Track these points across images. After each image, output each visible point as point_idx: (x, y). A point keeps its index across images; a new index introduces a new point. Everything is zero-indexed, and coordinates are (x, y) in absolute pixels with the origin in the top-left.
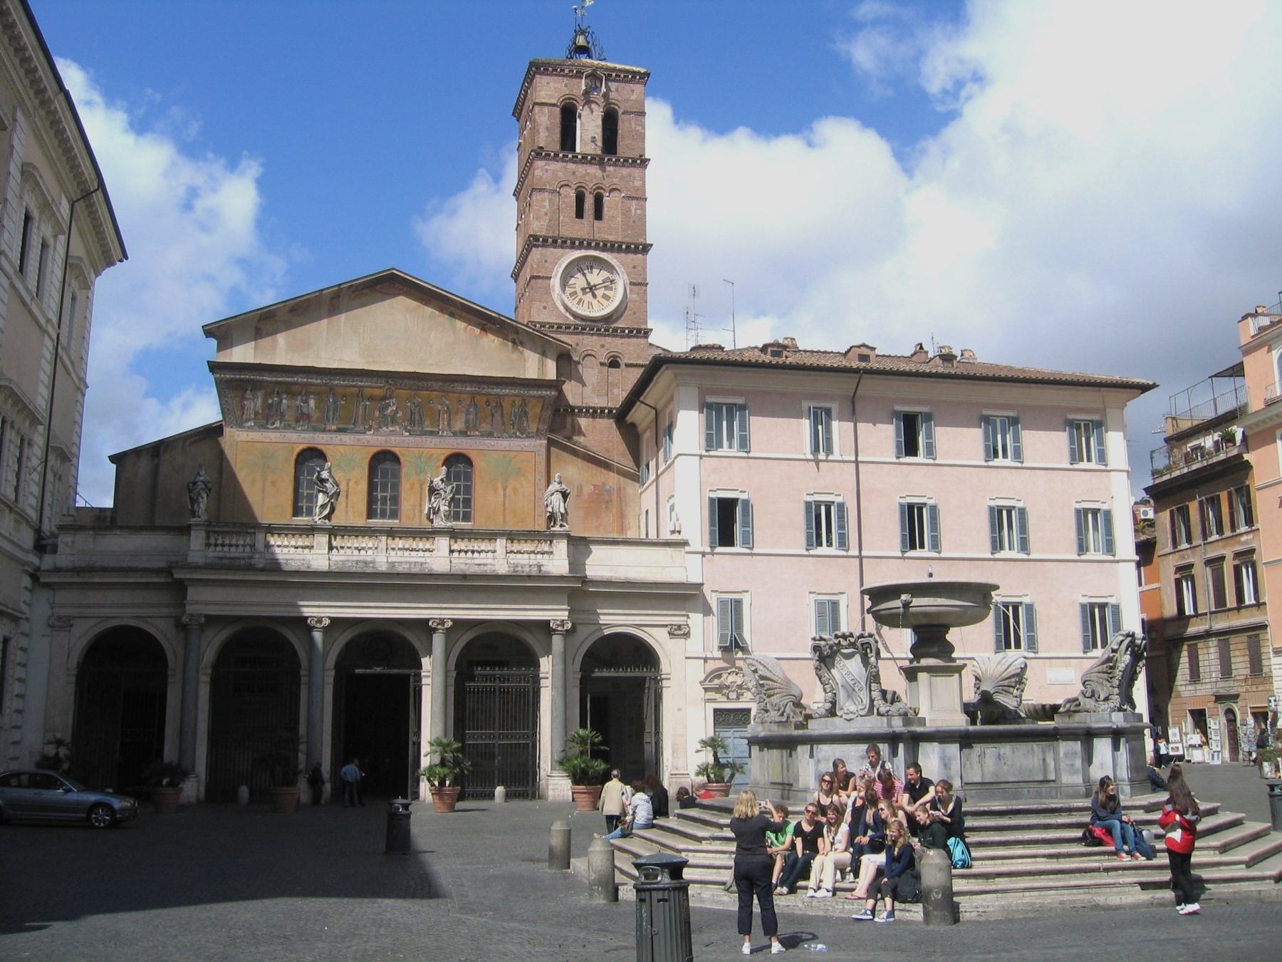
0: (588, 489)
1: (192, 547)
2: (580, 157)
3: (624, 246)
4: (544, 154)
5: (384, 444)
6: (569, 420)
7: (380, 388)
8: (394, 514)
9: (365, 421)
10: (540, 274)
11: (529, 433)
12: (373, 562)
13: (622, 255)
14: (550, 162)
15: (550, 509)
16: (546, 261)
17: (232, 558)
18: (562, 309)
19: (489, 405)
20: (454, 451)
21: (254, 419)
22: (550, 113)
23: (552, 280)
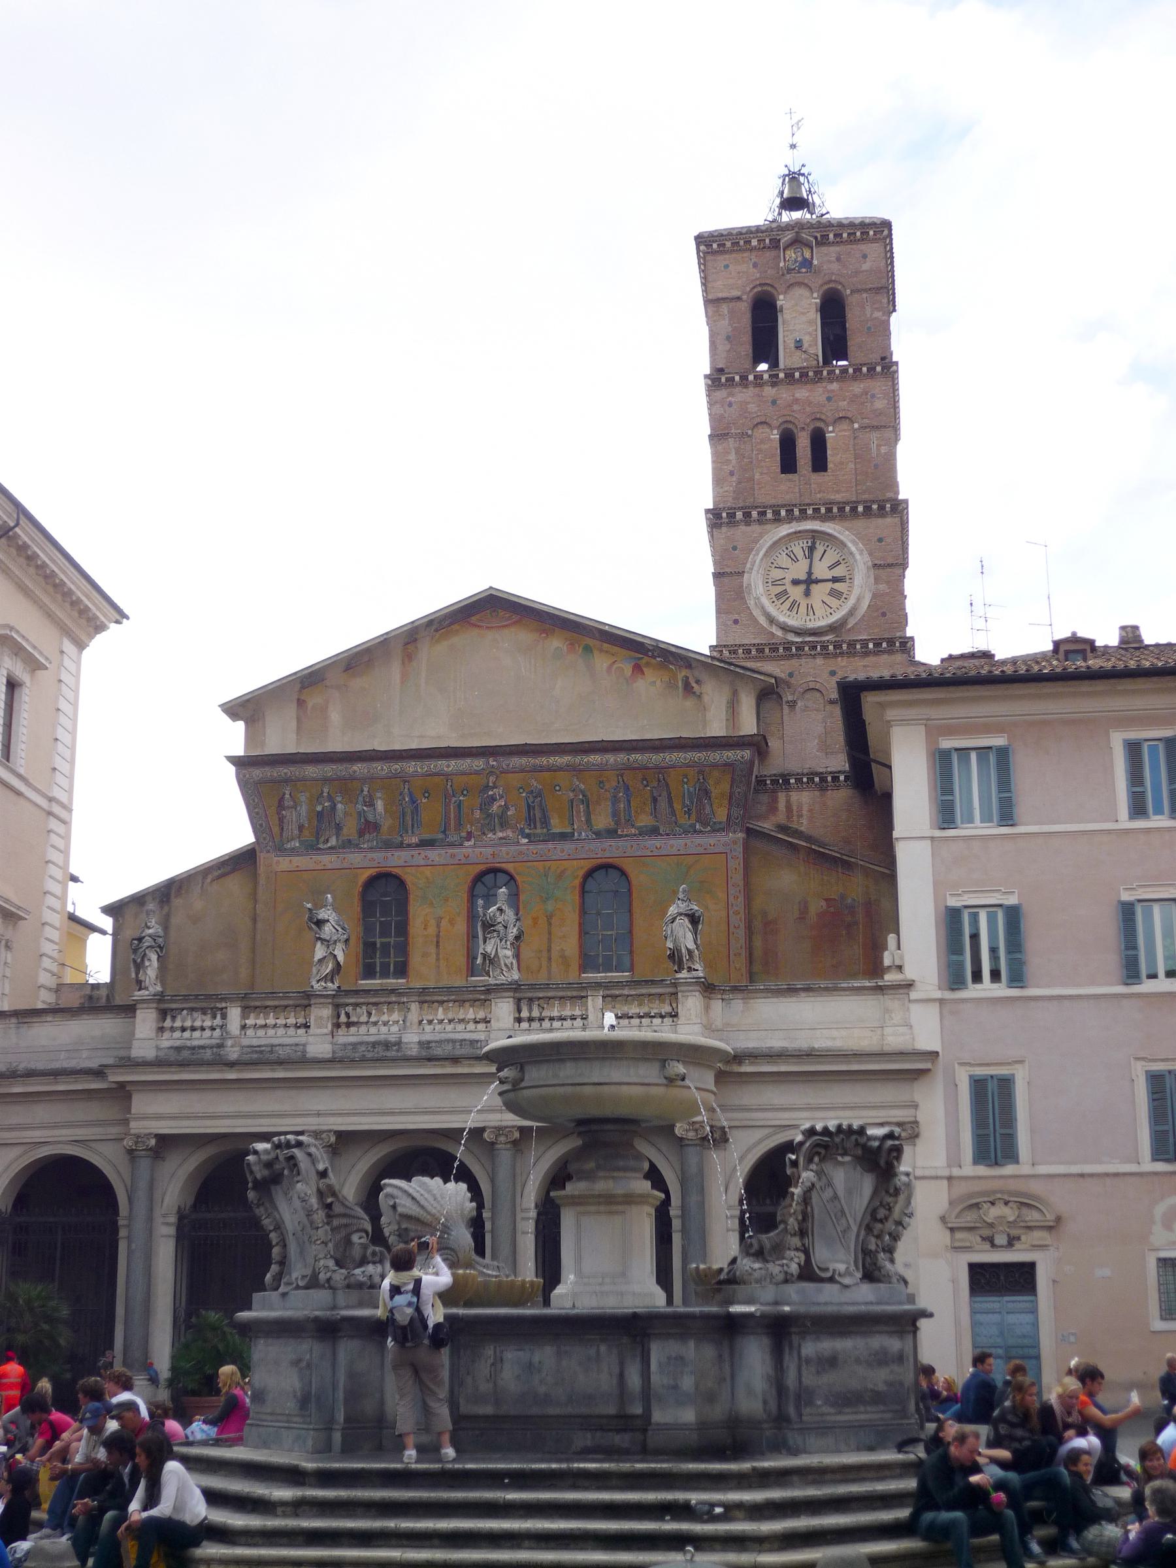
0: (816, 906)
1: (138, 1035)
2: (782, 375)
3: (860, 509)
4: (723, 380)
5: (491, 859)
6: (782, 797)
7: (477, 773)
8: (402, 970)
9: (459, 826)
10: (728, 570)
11: (715, 823)
12: (399, 1043)
13: (860, 523)
14: (737, 389)
15: (670, 945)
16: (735, 548)
17: (193, 1048)
18: (762, 620)
20: (600, 861)
21: (299, 837)
22: (732, 312)
23: (746, 575)
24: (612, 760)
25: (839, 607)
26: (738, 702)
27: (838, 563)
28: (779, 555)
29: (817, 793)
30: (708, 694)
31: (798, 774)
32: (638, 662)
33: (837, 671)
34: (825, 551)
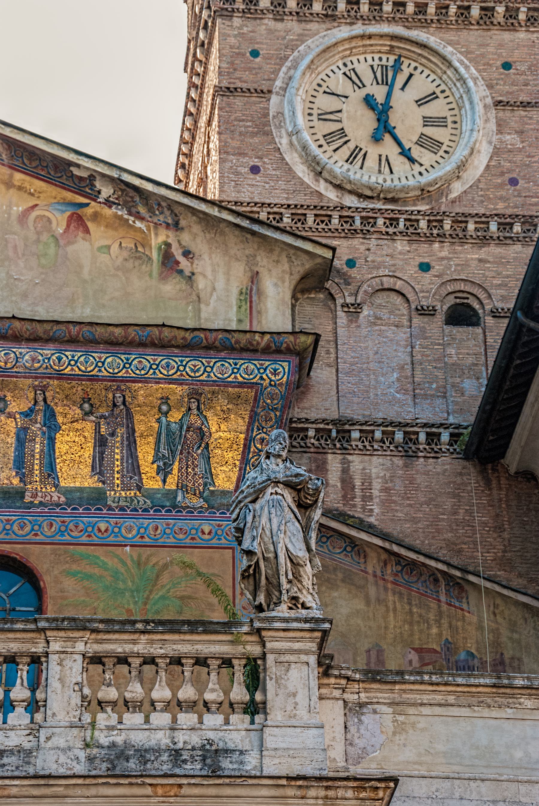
10: (239, 85)
11: (212, 492)
16: (255, 54)
19: (91, 413)
23: (274, 99)
24: (27, 357)
25: (435, 164)
26: (260, 293)
27: (433, 96)
28: (331, 74)
29: (399, 462)
30: (205, 276)
31: (366, 423)
32: (79, 212)
33: (433, 264)
34: (411, 75)
